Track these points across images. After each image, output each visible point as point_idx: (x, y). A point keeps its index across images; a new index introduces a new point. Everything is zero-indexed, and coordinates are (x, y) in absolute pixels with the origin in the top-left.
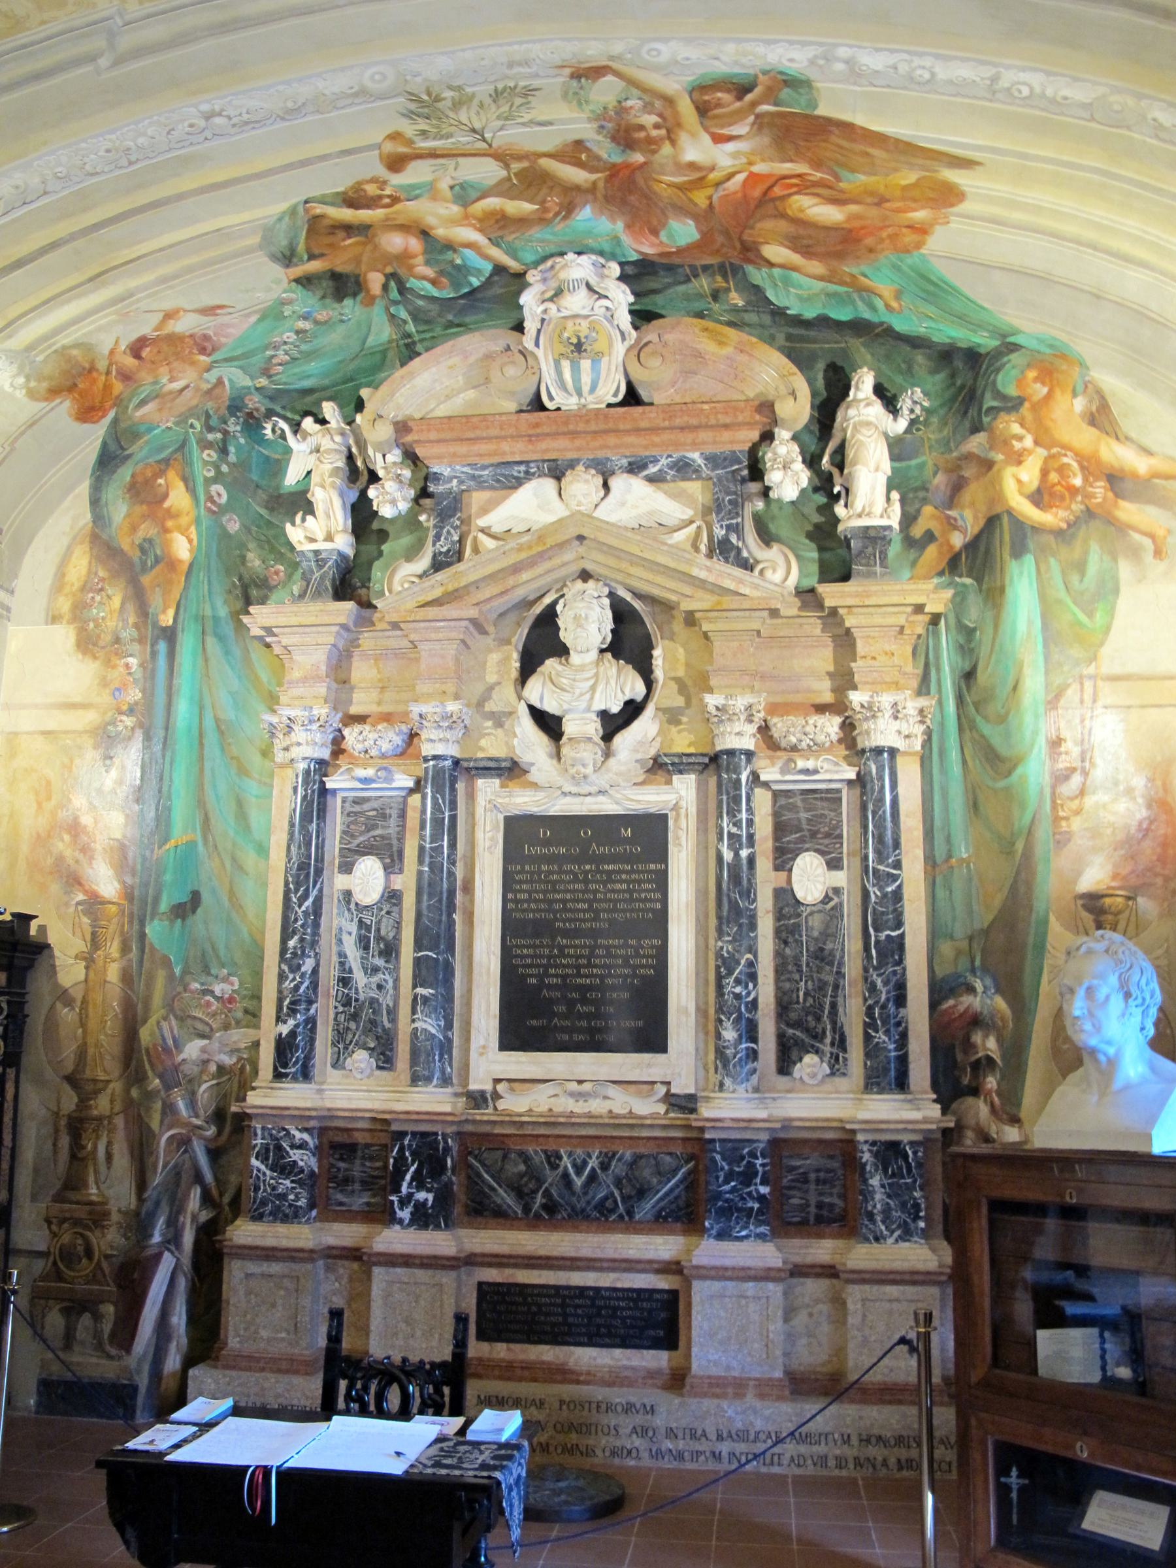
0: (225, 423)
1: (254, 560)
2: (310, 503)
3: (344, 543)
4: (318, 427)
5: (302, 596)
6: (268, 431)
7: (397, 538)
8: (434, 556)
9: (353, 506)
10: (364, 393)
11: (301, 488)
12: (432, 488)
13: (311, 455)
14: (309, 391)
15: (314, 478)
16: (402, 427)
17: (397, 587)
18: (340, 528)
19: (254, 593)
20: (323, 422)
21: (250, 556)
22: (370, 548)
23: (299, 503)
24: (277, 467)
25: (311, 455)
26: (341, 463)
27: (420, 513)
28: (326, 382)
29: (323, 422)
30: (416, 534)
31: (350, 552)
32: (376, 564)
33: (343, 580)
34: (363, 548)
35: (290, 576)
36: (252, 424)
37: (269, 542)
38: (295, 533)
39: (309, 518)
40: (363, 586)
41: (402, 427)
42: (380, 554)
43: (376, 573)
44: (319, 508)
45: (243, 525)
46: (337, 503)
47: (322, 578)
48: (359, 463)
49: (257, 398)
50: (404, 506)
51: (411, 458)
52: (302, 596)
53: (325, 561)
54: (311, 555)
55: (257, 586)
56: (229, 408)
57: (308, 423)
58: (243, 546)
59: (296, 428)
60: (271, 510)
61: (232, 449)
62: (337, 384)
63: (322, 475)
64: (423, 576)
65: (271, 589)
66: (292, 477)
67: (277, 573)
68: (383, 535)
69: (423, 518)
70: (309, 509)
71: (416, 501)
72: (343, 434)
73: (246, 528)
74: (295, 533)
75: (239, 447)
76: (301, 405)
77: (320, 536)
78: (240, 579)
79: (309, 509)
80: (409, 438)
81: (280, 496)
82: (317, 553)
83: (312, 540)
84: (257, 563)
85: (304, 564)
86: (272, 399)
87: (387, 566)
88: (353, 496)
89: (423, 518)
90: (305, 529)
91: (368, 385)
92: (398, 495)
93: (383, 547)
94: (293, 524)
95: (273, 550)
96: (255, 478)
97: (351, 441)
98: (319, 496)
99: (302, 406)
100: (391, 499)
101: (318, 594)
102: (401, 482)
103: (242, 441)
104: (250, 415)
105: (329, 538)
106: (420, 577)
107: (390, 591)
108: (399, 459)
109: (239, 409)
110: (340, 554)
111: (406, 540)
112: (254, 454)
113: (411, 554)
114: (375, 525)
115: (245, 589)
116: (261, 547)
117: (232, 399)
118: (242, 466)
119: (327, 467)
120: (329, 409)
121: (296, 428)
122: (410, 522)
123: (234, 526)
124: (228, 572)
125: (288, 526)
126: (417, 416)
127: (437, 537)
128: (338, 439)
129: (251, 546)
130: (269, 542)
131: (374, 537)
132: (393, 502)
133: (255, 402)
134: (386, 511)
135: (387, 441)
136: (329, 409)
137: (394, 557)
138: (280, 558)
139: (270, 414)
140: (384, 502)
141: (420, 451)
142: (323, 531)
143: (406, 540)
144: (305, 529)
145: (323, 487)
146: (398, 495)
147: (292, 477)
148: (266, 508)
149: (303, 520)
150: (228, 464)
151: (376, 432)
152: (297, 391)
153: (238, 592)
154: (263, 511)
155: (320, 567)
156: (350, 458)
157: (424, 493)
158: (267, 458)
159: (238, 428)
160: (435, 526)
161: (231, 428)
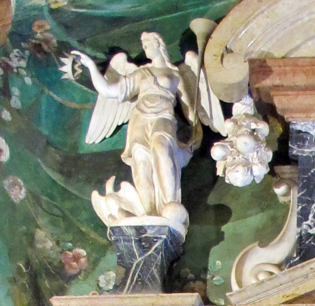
0: (7, 55)
1: (45, 241)
2: (129, 168)
3: (174, 218)
4: (132, 67)
5: (118, 287)
6: (67, 68)
7: (245, 217)
8: (300, 239)
9: (184, 170)
10: (198, 26)
11: (107, 147)
12: (295, 150)
13: (126, 104)
14: (116, 21)
15: (132, 133)
16: (260, 67)
17: (249, 279)
18: (170, 199)
19: (46, 284)
20: (141, 60)
21: (40, 234)
22: (208, 228)
23: (111, 166)
24: (74, 120)
25: (126, 104)
26: (169, 115)
27: (278, 185)
28: (143, 8)
29: (141, 60)
30: (271, 212)
31: (182, 231)
32: (215, 251)
33: (170, 270)
34: (197, 228)
35: (94, 263)
36: (44, 60)
37: (64, 218)
38: (107, 205)
39: (125, 185)
40: (197, 278)
41: (260, 67)
42: (220, 237)
43: (215, 262)
44: (139, 174)
45: (29, 192)
46: (166, 166)
47: (147, 263)
48: (191, 117)
49: (49, 24)
50: (260, 171)
51: (266, 110)
52: (118, 287)
53: (151, 241)
54: (131, 232)
55: (49, 274)
56: (11, 35)
57: (119, 62)
58: (30, 221)
59: (103, 67)
60: (68, 175)
61: (15, 91)
62: (158, 14)
63: (144, 128)
64: (287, 263)
65: (71, 278)
66: (96, 132)
67: (76, 258)
68: (223, 213)
69: (280, 190)
70: (124, 174)
71: (272, 165)
72: (170, 76)
73: (33, 196)
74: (107, 205)
75: (23, 88)
76: (104, 40)
77: (140, 207)
78: (28, 264)
79: (124, 174)
80: (268, 82)
81: (79, 157)
82: (140, 230)
83: (129, 214)
84: (50, 244)
85: (122, 245)
86: (68, 27)
87: (231, 254)
88: (185, 158)
89: (280, 190)
90: (119, 199)
91: (201, 15)
92: (253, 157)
93: (224, 228)
94: (102, 192)
95: (70, 227)
96: (45, 132)
97: (180, 87)
98: (137, 155)
99: (113, 39)
100: (241, 160)
101: (141, 285)
102: (256, 139)
103: (28, 80)
104: (38, 47)
105: (153, 211)
106: (280, 266)
107: (239, 283)
108: (251, 111)
109: (25, 39)
110: (172, 234)
111: (256, 220)
112: (44, 100)
113: (267, 235)
114: (212, 199)
115: (34, 277)
116: (53, 223)
117: (17, 23)
118: (28, 113)
119: (151, 118)
120: (152, 44)
121: (103, 67)
122: (261, 195)
123: (19, 194)
124: (12, 255)
125: (95, 195)
126: (278, 54)
127: (303, 216)
128: (164, 82)
129: (41, 221)
130: (64, 218)
131: (211, 214)
132: (248, 165)
133: (46, 31)
134: (237, 178)
135: (239, 84)
136: (152, 44)
137: (241, 244)
138: (81, 239)
139: (64, 49)
140: (235, 164)
141: (280, 102)
142: (145, 201)
143: (256, 220)
144: (119, 199)
145: (145, 143)
146: (253, 157)
147: (96, 132)
148: (61, 172)
149: (117, 187)
150: (10, 109)
151: (220, 73)
152: (102, 18)
153: (25, 281)
154: (56, 177)
155: (144, 249)
156: (179, 110)
157: (282, 156)
158: (61, 106)
159: (23, 63)
160: (300, 200)
161: (14, 63)
